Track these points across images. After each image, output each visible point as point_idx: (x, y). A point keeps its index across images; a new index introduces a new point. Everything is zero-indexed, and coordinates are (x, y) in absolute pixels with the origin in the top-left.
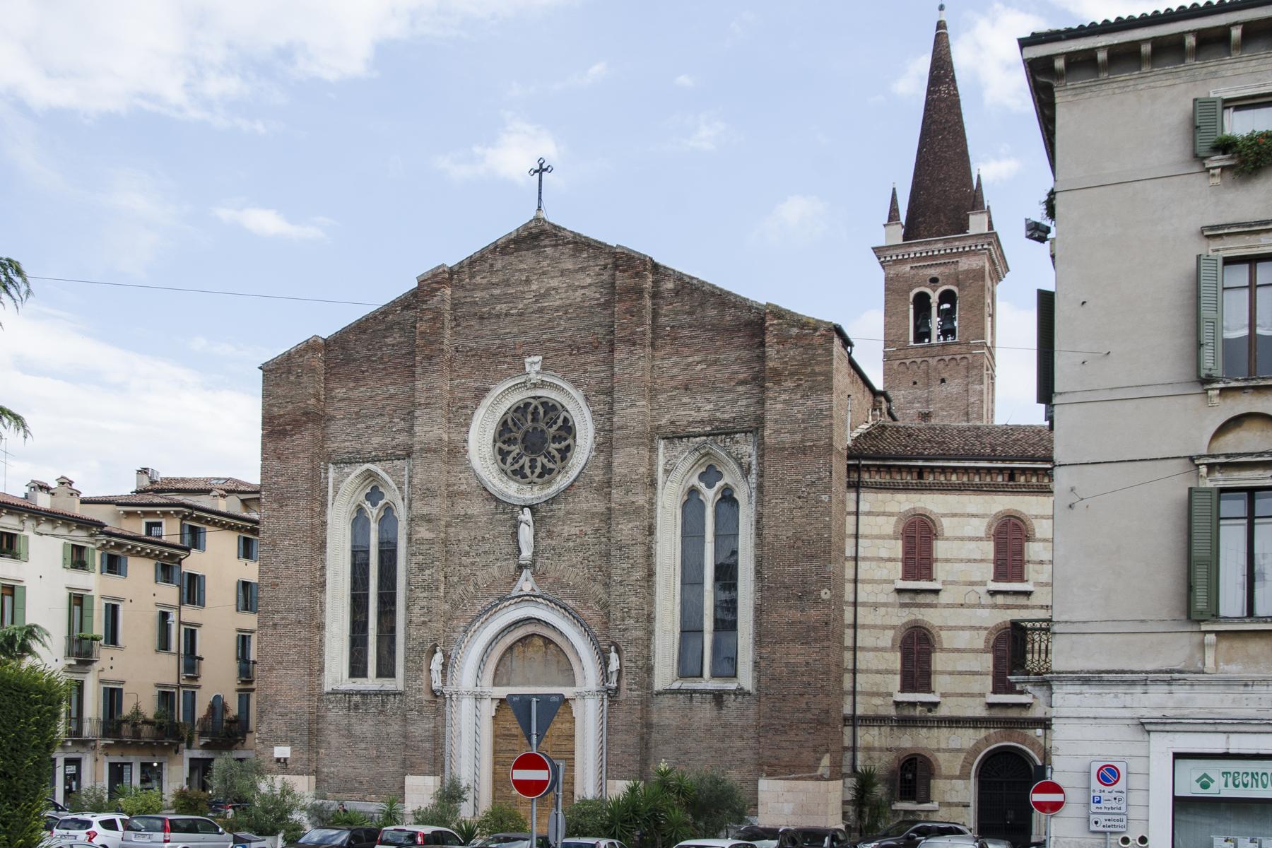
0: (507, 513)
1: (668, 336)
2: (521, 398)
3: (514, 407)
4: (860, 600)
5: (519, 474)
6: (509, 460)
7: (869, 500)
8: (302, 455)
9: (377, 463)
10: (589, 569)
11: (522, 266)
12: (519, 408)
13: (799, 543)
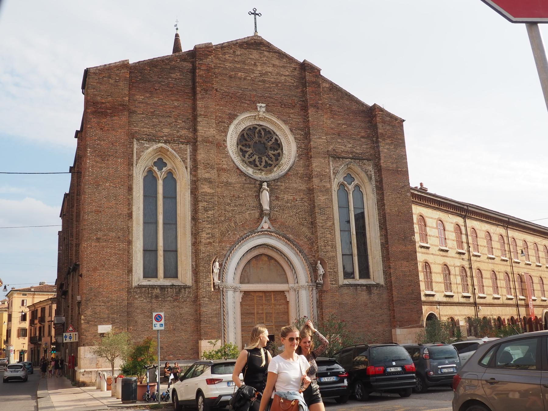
0: (252, 184)
2: (251, 124)
3: (248, 128)
5: (253, 164)
6: (247, 156)
8: (120, 131)
10: (299, 219)
11: (251, 57)
12: (250, 129)
13: (400, 214)
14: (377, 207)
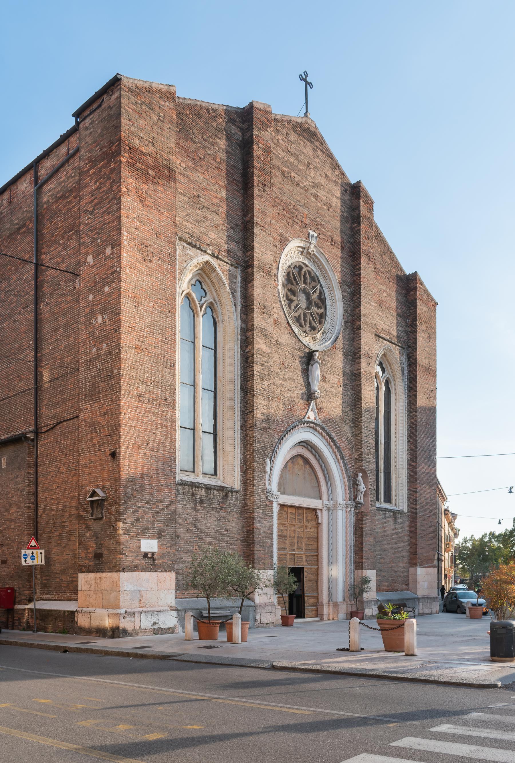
9: (215, 259)
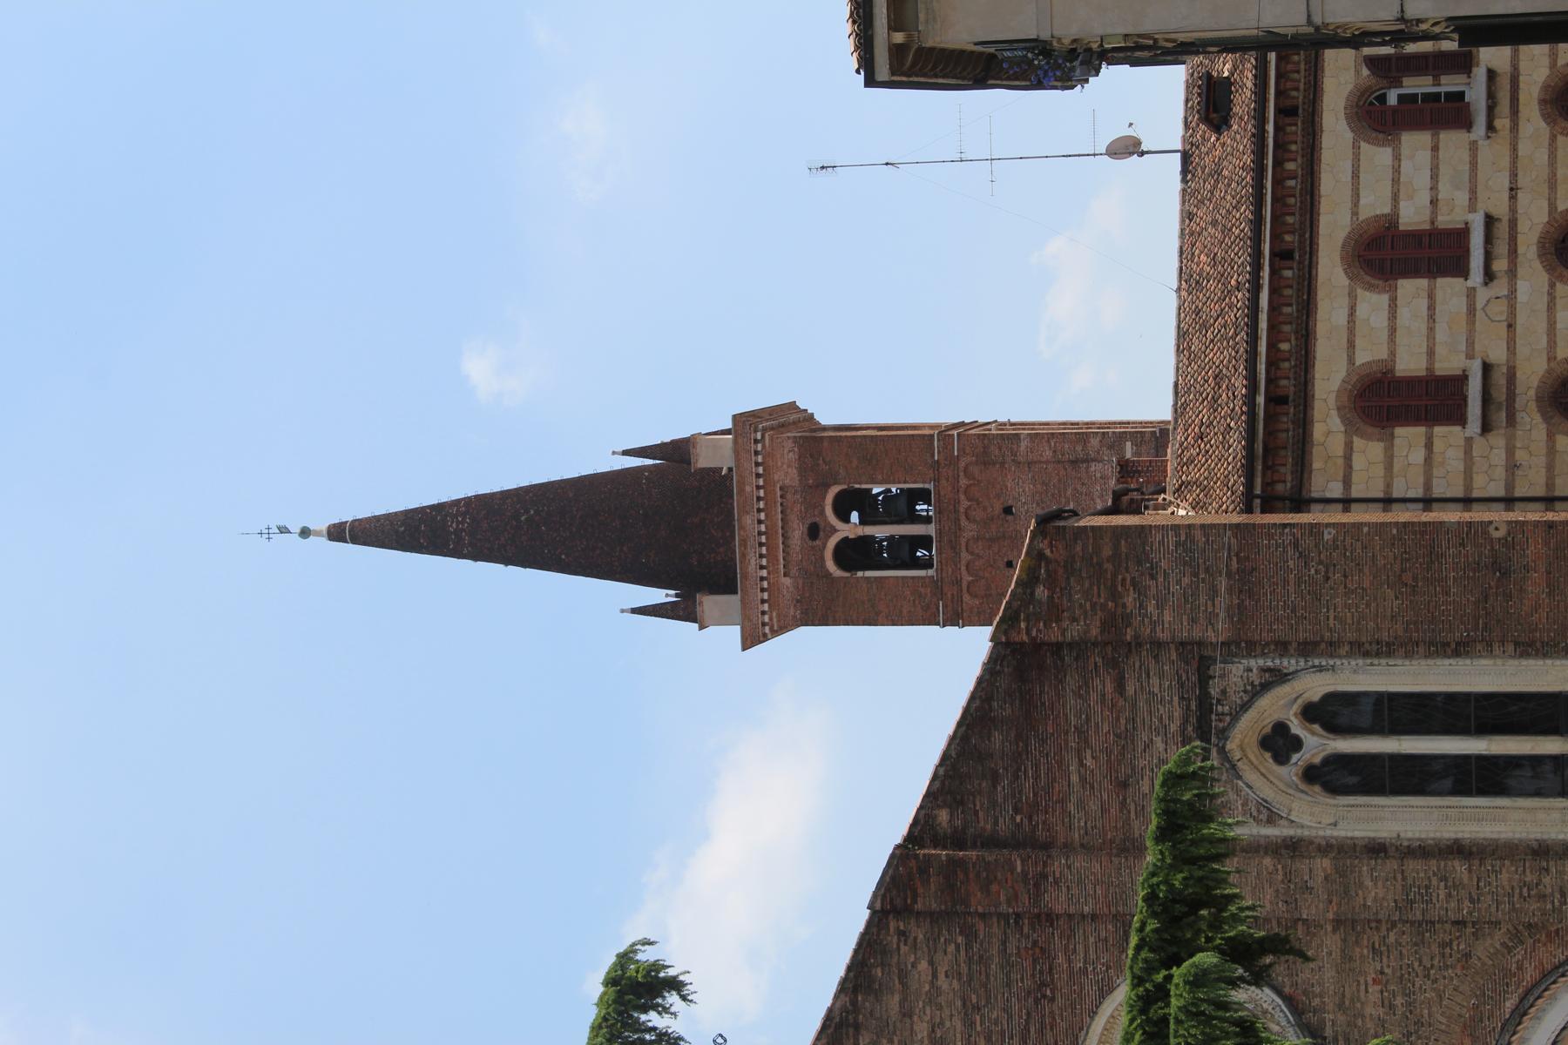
1: (1030, 819)
4: (1501, 493)
7: (1325, 483)
10: (1446, 967)
13: (1408, 578)
14: (1383, 661)
